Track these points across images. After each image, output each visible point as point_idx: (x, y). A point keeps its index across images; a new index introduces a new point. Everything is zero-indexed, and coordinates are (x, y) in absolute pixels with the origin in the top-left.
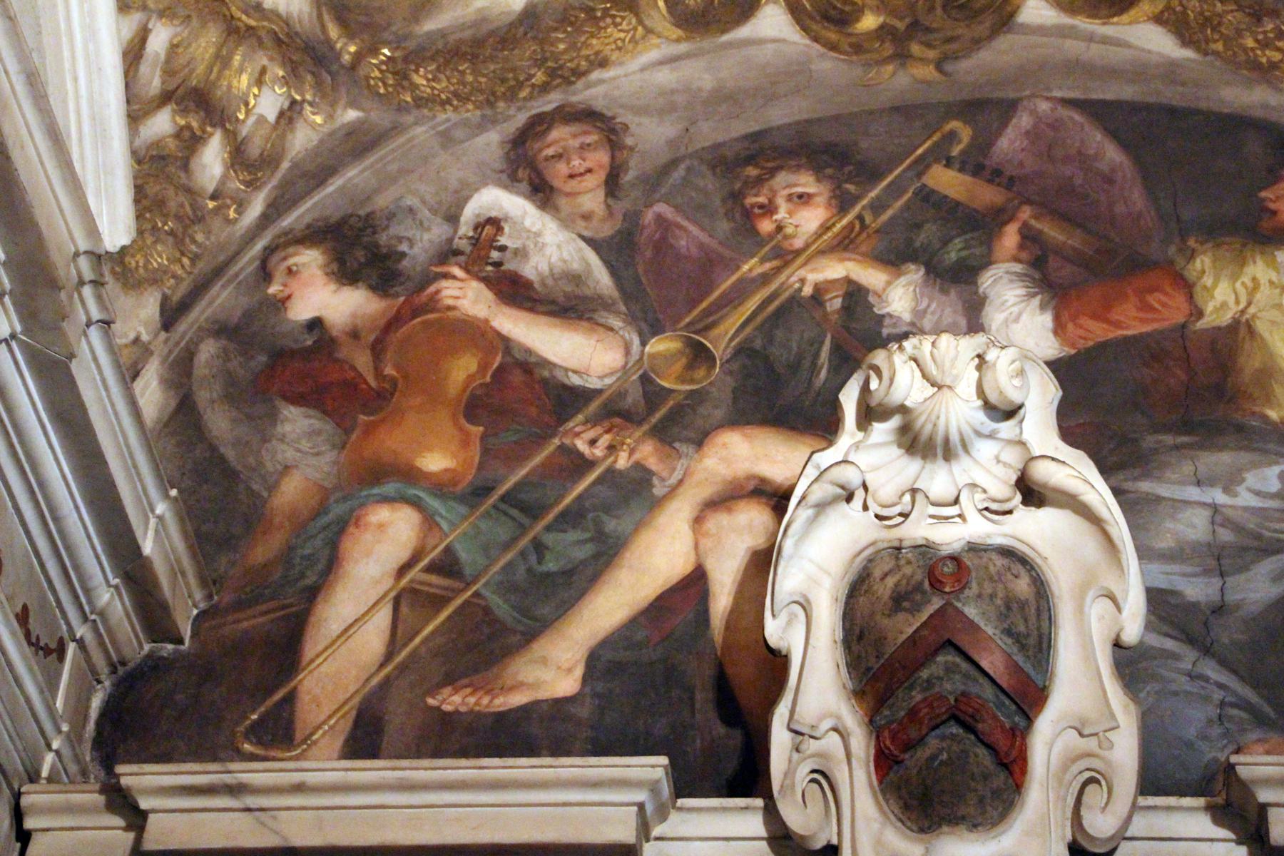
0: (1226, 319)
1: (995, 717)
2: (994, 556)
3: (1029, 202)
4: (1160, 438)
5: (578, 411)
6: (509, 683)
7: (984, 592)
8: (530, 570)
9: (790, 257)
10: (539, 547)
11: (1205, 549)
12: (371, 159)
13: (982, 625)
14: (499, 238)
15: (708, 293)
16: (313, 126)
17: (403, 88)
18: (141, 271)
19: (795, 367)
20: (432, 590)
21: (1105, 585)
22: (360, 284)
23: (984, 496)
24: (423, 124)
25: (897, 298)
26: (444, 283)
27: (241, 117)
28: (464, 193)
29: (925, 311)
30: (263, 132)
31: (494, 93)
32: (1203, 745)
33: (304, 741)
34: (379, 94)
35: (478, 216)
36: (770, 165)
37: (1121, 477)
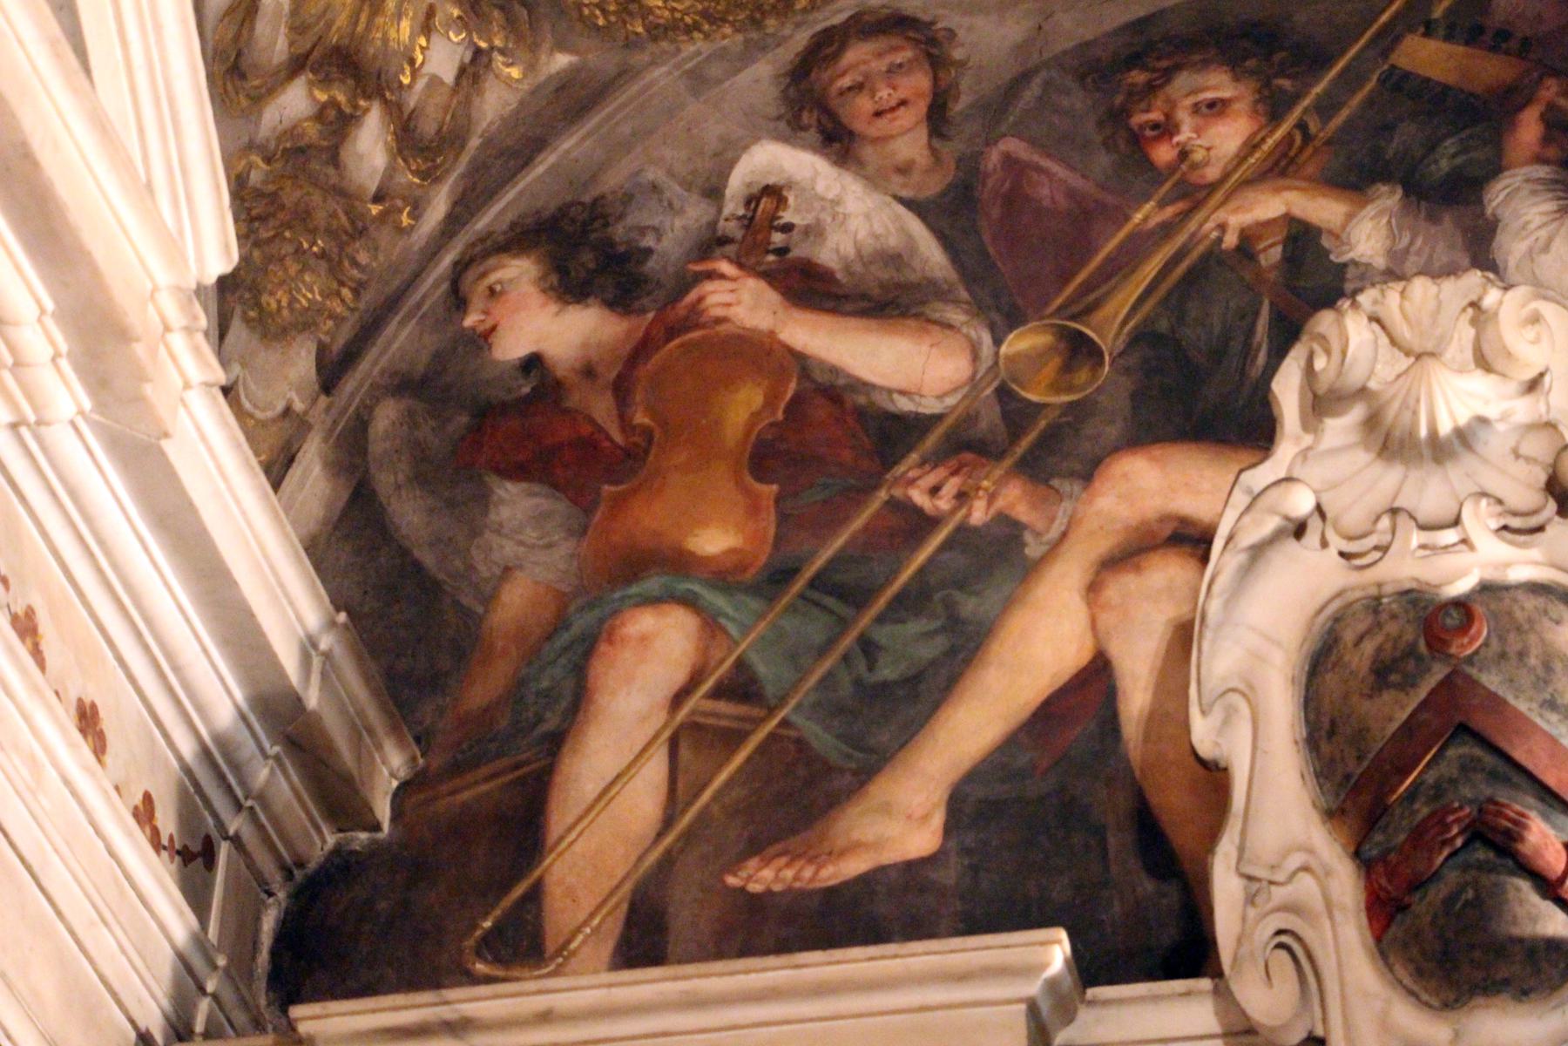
3: (1555, 73)
5: (910, 449)
6: (841, 842)
8: (858, 683)
9: (1200, 195)
10: (868, 647)
12: (594, 120)
14: (781, 213)
15: (1083, 263)
16: (508, 82)
17: (630, 14)
18: (285, 313)
19: (1218, 354)
20: (724, 723)
22: (590, 300)
24: (664, 63)
25: (1364, 237)
26: (709, 286)
27: (406, 80)
28: (730, 155)
29: (1407, 251)
30: (440, 98)
31: (759, 8)
33: (559, 953)
34: (598, 28)
35: (749, 185)
36: (1164, 64)
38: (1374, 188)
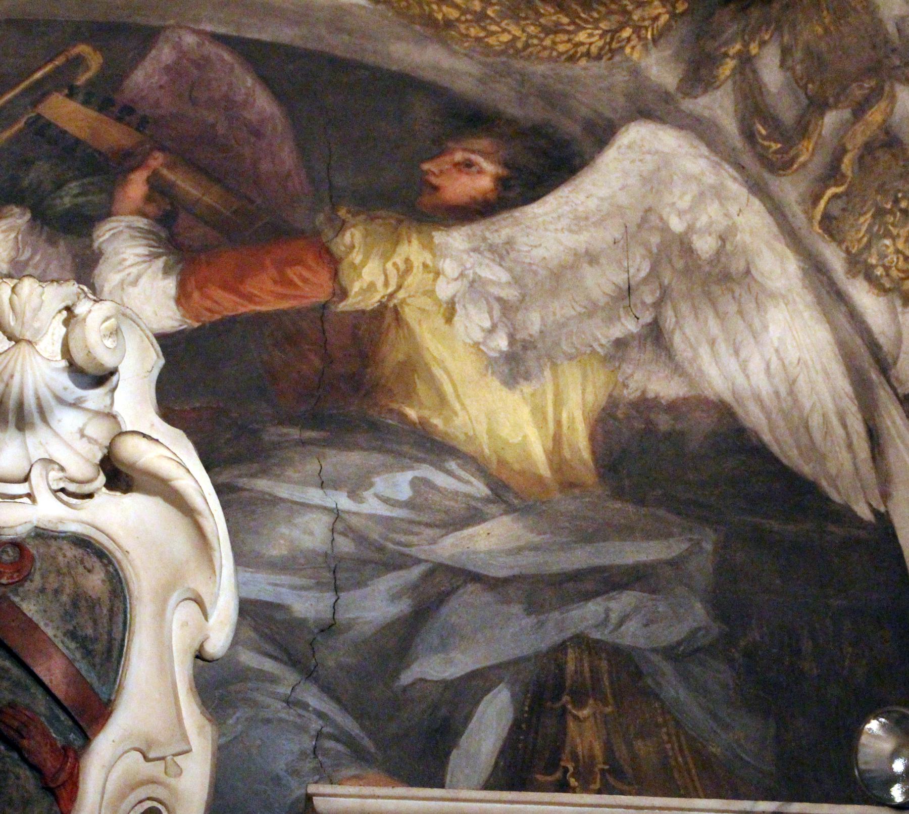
0: (372, 302)
1: (46, 735)
2: (66, 546)
3: (162, 149)
4: (285, 430)
7: (47, 586)
11: (320, 559)
13: (42, 625)
21: (192, 586)
23: (61, 474)
29: (26, 263)
32: (293, 783)
37: (236, 472)
38: (9, 208)
